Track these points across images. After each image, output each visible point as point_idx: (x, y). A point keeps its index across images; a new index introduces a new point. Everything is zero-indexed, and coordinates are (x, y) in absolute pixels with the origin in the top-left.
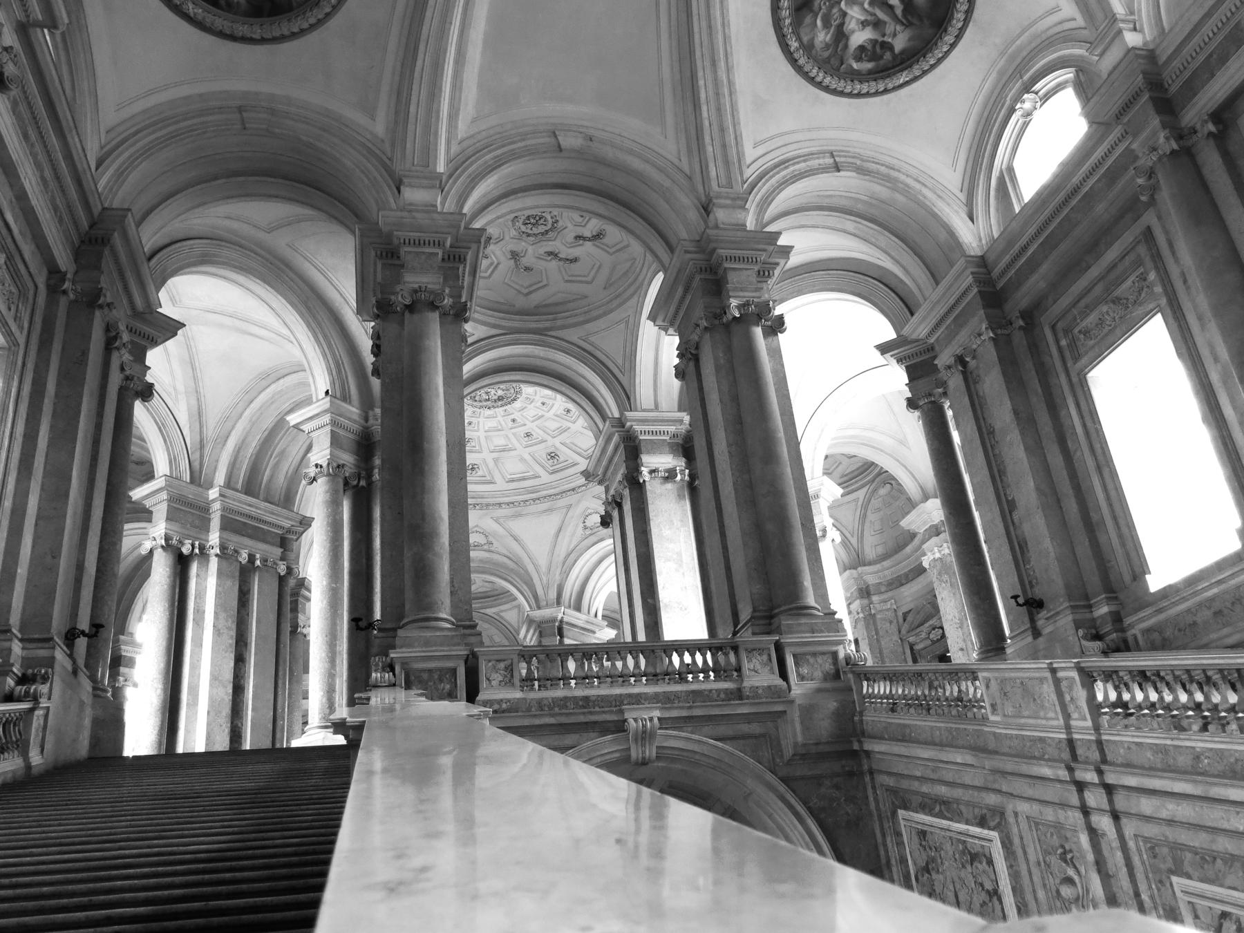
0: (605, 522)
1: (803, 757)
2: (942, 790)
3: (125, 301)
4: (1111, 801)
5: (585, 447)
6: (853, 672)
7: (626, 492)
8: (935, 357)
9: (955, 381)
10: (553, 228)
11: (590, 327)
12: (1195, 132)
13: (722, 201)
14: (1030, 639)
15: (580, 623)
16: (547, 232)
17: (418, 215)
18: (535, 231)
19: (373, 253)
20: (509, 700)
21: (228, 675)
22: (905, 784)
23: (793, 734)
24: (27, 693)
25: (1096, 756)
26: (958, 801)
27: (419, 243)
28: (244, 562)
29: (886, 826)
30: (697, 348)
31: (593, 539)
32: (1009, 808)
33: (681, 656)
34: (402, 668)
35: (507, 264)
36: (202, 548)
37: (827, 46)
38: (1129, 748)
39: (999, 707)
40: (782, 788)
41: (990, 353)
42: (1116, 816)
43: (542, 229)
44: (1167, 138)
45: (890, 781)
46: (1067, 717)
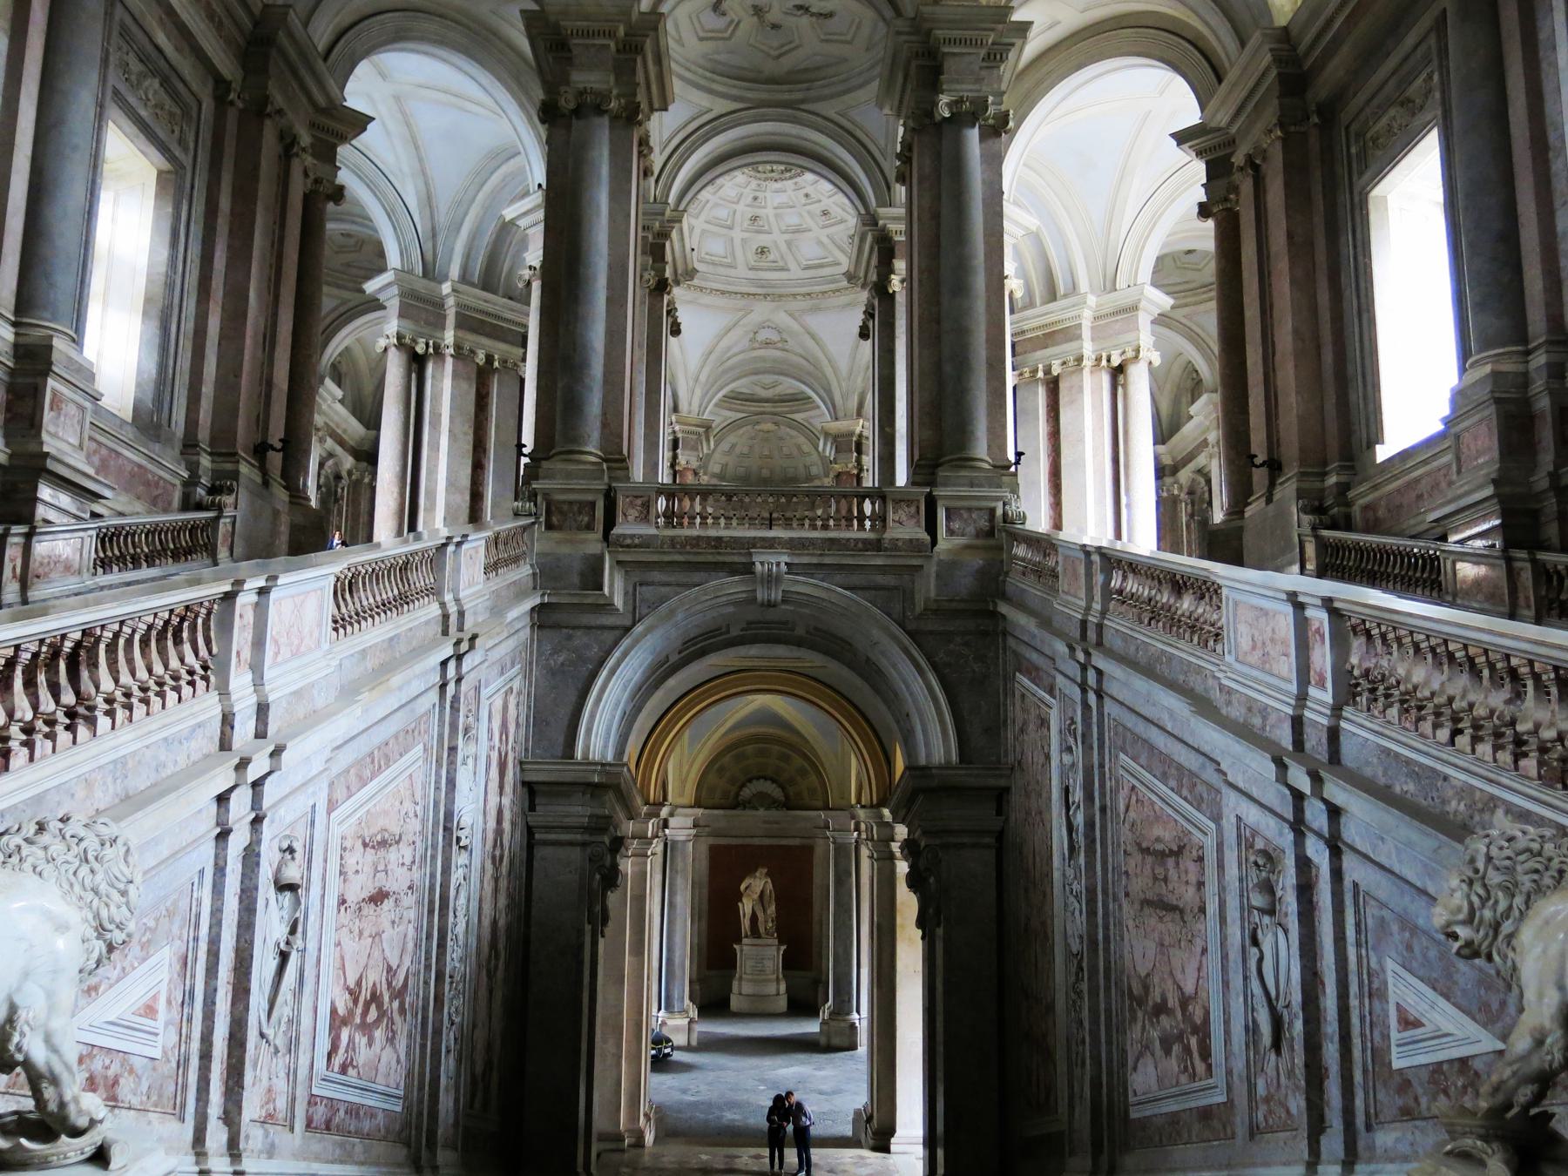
0: (864, 334)
1: (936, 612)
3: (304, 100)
7: (876, 303)
8: (1232, 154)
9: (1247, 186)
11: (846, 98)
20: (641, 536)
23: (927, 588)
24: (213, 502)
27: (587, 34)
35: (748, 22)
40: (906, 640)
42: (1100, 695)
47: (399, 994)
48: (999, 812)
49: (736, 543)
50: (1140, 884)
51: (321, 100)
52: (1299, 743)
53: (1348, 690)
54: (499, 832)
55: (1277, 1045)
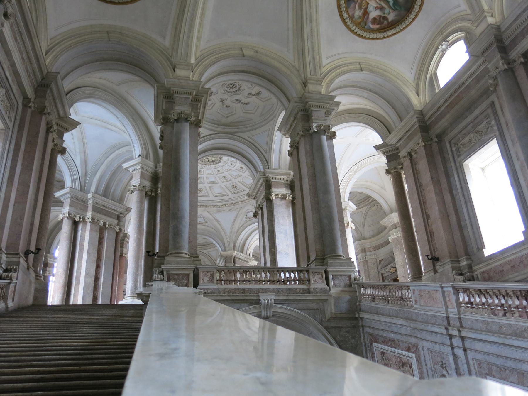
0: (255, 215)
2: (392, 335)
4: (463, 344)
5: (248, 184)
6: (357, 284)
7: (265, 204)
8: (399, 152)
9: (407, 163)
10: (239, 90)
11: (252, 132)
12: (515, 62)
13: (312, 81)
14: (433, 274)
15: (243, 258)
16: (236, 91)
17: (181, 81)
18: (231, 90)
19: (162, 97)
20: (211, 289)
21: (93, 273)
22: (376, 332)
23: (331, 309)
24: (8, 276)
25: (458, 324)
26: (398, 340)
28: (101, 225)
29: (368, 349)
30: (298, 143)
31: (249, 223)
32: (421, 343)
33: (285, 274)
34: (167, 273)
35: (219, 104)
36: (84, 219)
37: (360, 17)
38: (472, 322)
39: (418, 301)
40: (325, 331)
41: (422, 152)
42: (465, 350)
43: (234, 90)
44: (503, 64)
45: (371, 331)
46: (447, 307)
49: (251, 291)
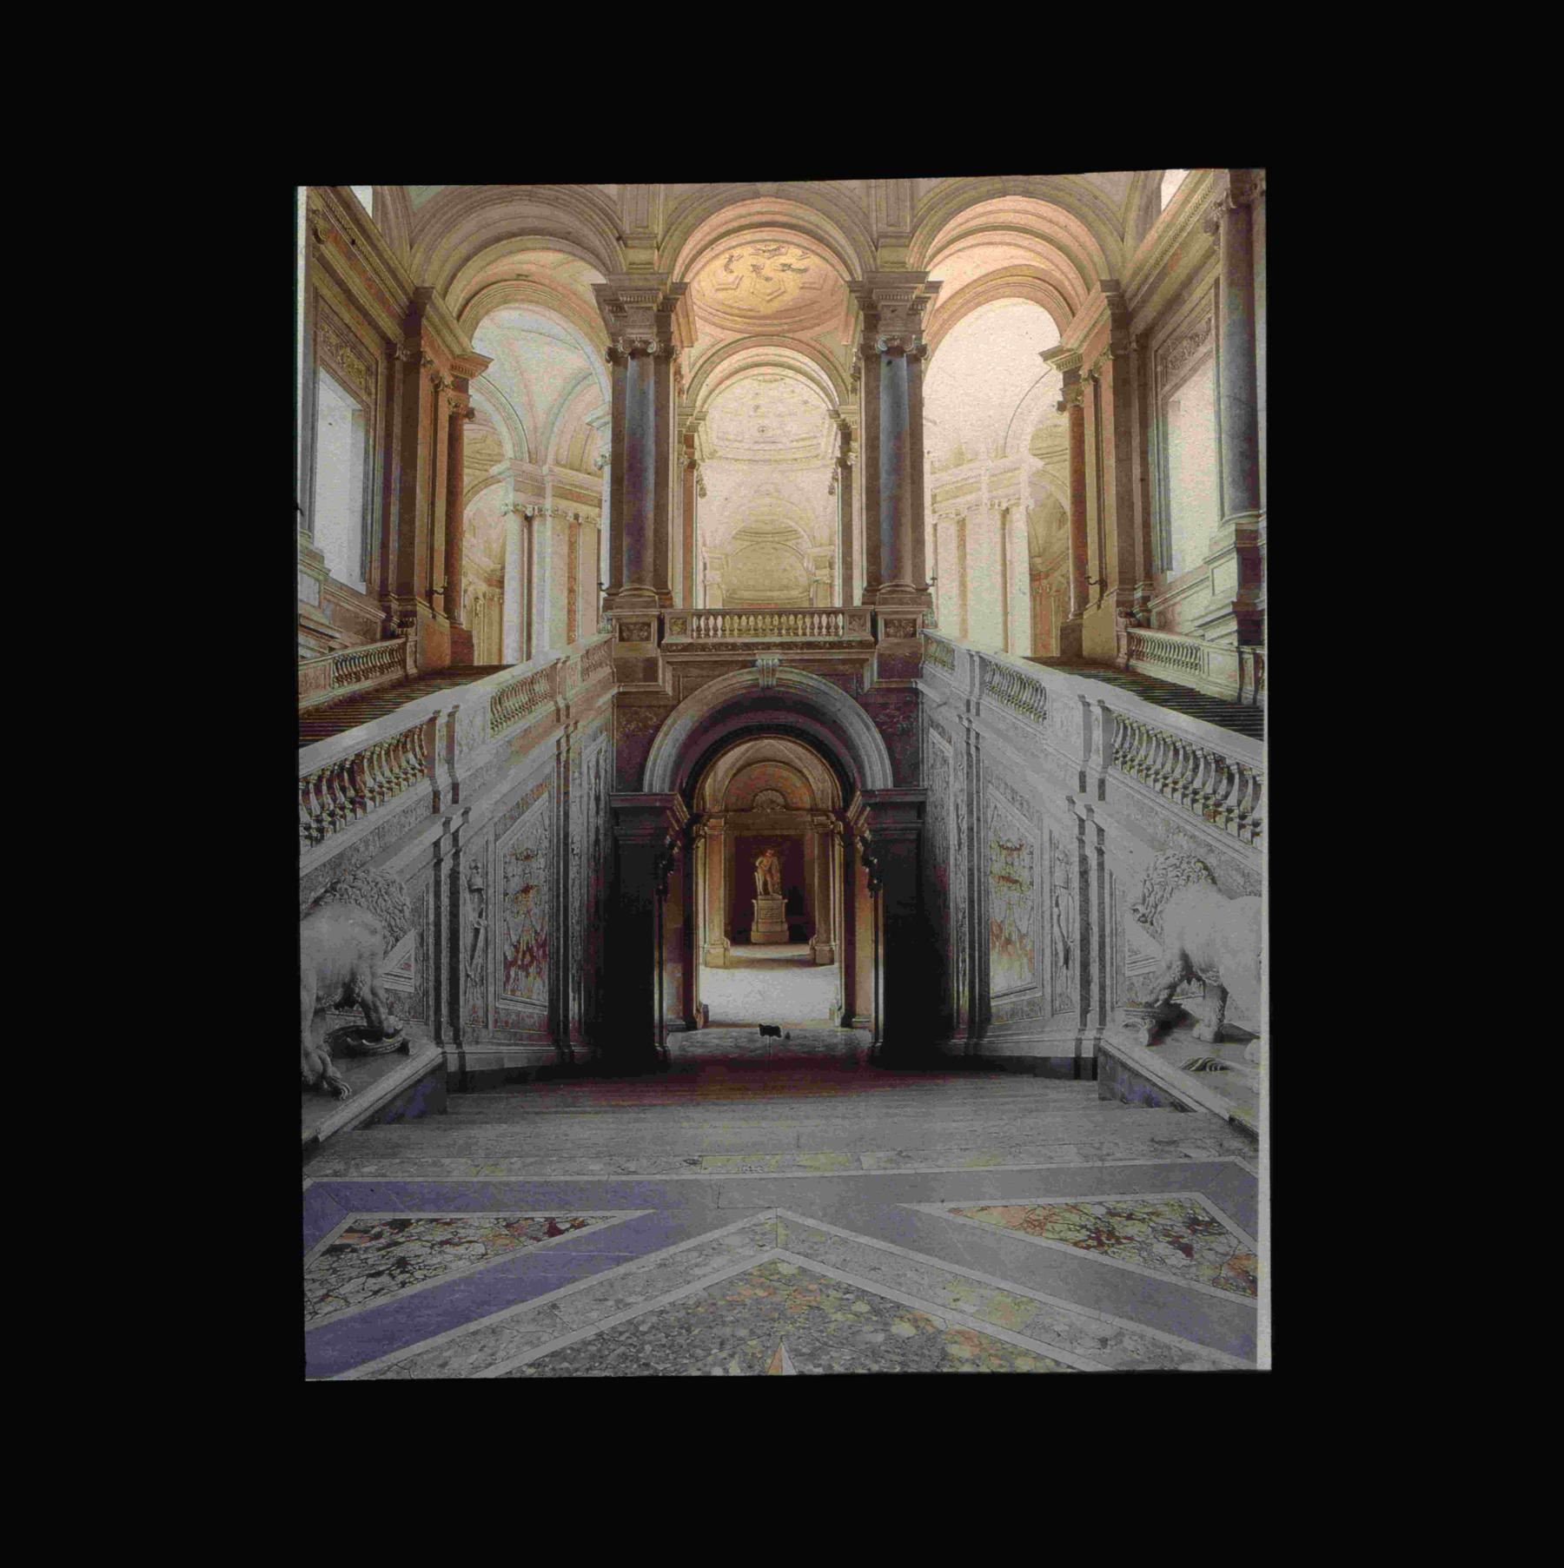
0: (831, 493)
9: (1088, 390)
36: (540, 510)
47: (543, 945)
48: (919, 817)
50: (997, 868)
51: (458, 351)
52: (1083, 788)
53: (1114, 756)
54: (597, 842)
55: (1066, 962)
